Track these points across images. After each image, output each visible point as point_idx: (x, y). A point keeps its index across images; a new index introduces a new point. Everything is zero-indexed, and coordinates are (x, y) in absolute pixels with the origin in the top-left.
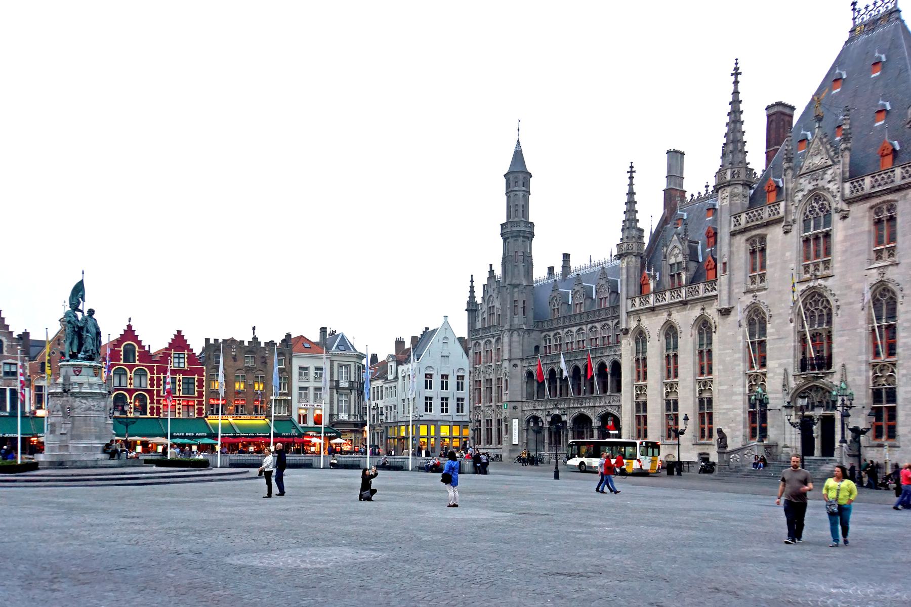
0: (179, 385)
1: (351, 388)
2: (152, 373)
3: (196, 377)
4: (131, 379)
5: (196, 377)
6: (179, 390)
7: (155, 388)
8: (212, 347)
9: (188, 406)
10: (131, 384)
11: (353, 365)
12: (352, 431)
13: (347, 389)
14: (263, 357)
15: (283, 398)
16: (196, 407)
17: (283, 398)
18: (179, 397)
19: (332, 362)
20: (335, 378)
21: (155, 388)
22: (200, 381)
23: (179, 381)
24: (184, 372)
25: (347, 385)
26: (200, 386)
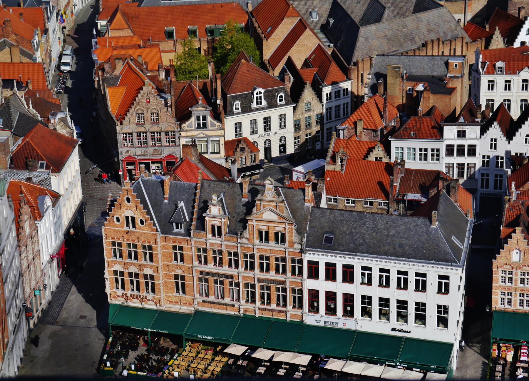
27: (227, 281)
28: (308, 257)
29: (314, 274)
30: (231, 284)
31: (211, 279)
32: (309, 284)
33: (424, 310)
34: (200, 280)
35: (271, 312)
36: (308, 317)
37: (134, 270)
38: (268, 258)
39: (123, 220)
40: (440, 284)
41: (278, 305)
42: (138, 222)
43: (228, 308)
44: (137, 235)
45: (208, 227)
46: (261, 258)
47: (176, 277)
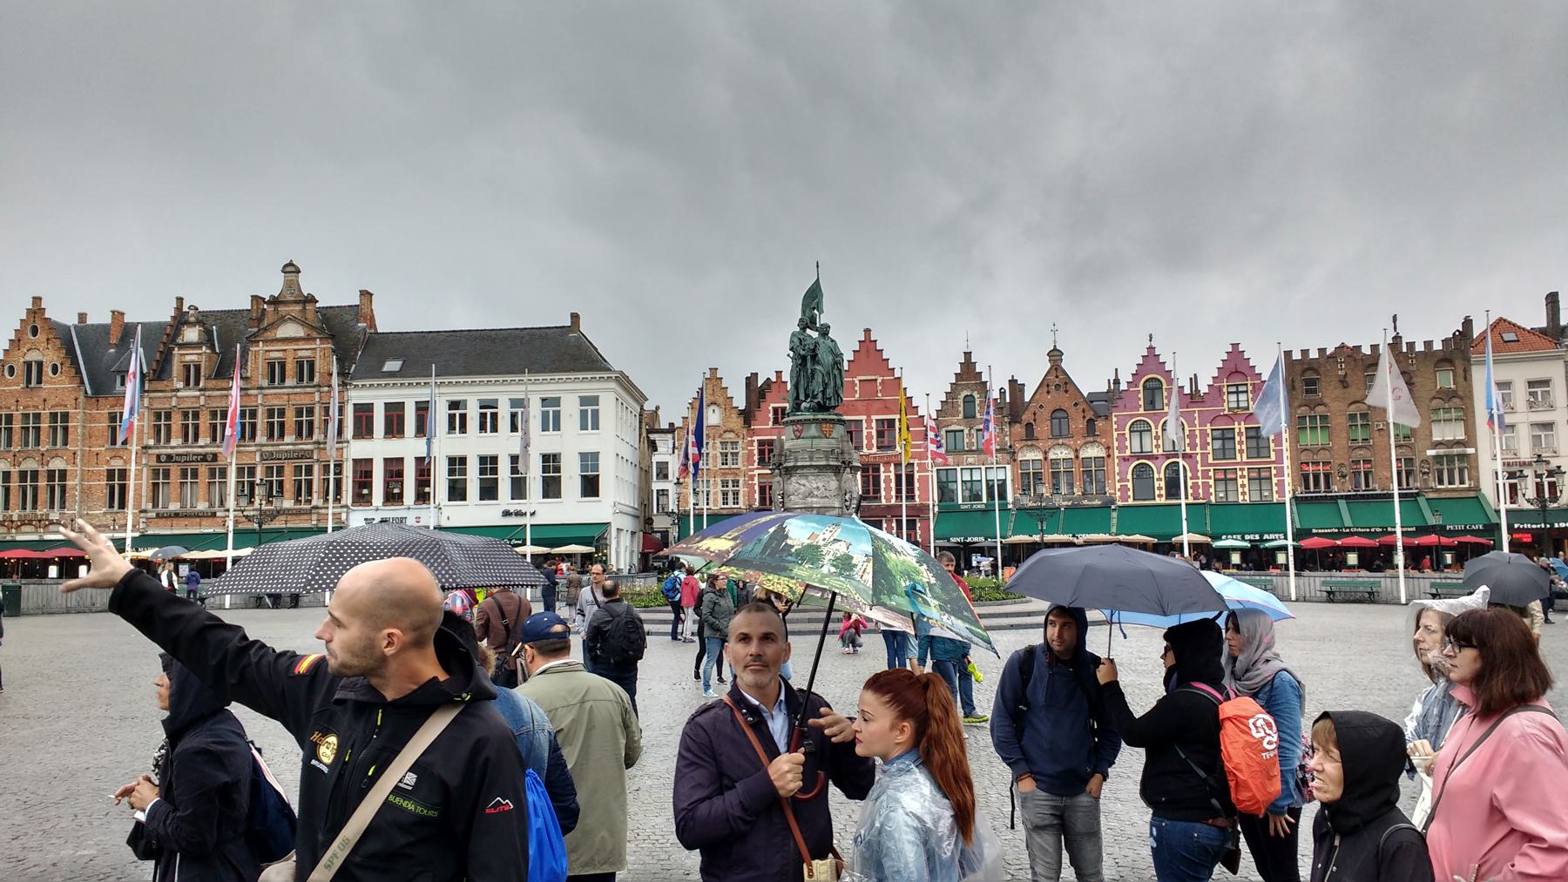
0: (1241, 443)
2: (1191, 424)
4: (1157, 438)
6: (1241, 451)
7: (1198, 450)
9: (1260, 479)
10: (1157, 446)
15: (1456, 450)
16: (1275, 480)
17: (1456, 450)
18: (1242, 463)
21: (1198, 450)
23: (1240, 434)
27: (203, 469)
28: (357, 396)
29: (364, 428)
30: (212, 473)
31: (175, 470)
32: (358, 449)
33: (557, 469)
34: (156, 473)
35: (283, 518)
36: (353, 516)
37: (29, 465)
38: (282, 413)
39: (20, 370)
40: (583, 414)
41: (298, 501)
42: (48, 370)
43: (205, 522)
44: (44, 394)
45: (176, 368)
46: (270, 413)
47: (110, 474)
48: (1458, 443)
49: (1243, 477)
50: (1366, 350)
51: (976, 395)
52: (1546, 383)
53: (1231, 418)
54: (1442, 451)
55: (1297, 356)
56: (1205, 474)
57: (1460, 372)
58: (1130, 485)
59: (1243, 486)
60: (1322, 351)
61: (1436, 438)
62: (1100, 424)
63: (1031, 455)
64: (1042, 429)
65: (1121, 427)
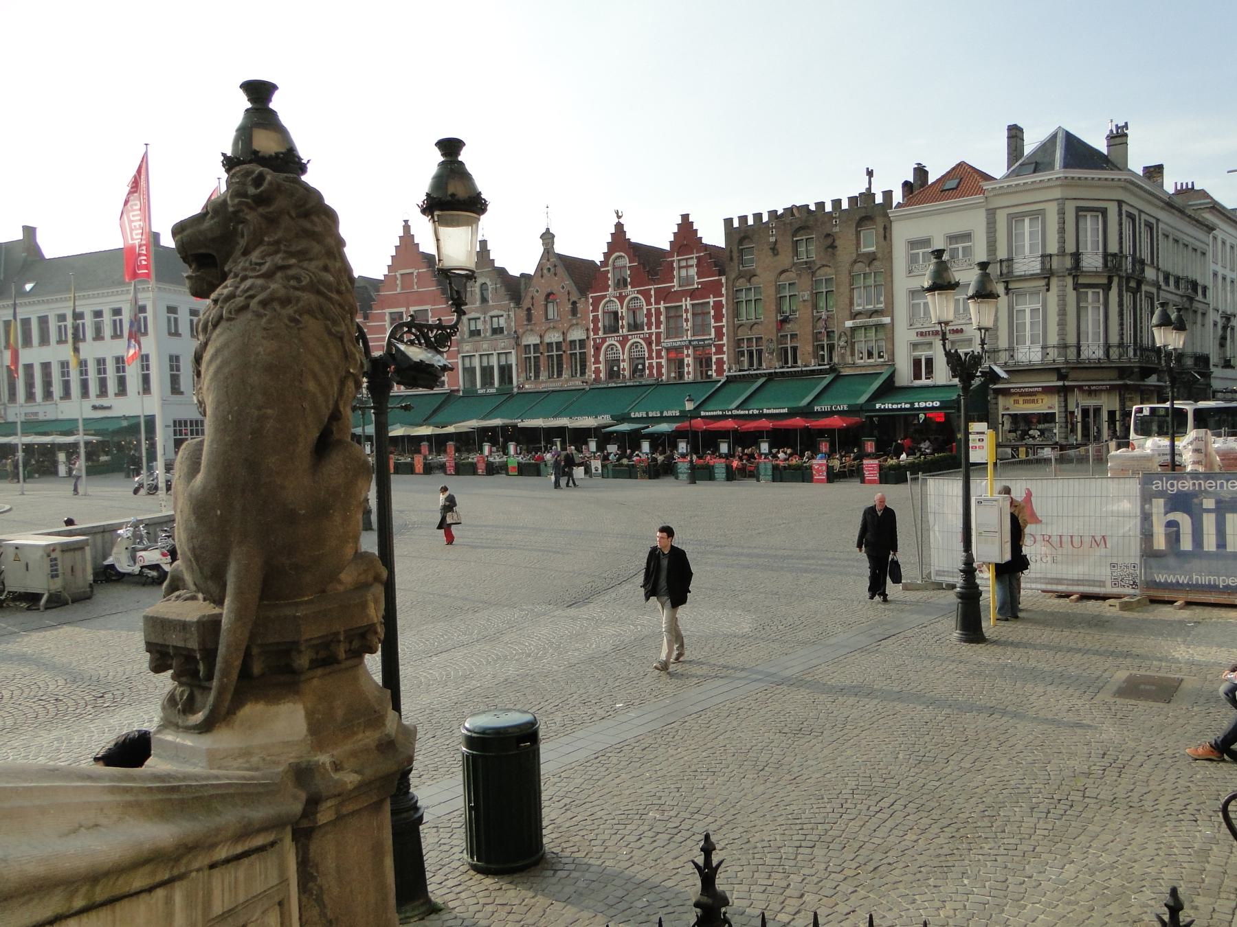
1: (1047, 275)
2: (649, 303)
3: (711, 300)
5: (711, 300)
7: (654, 330)
8: (743, 234)
11: (1052, 211)
12: (1048, 390)
13: (1033, 277)
14: (828, 235)
15: (874, 320)
17: (874, 320)
19: (991, 214)
20: (1002, 254)
21: (654, 330)
22: (718, 306)
24: (693, 294)
25: (1035, 267)
26: (718, 317)
36: (9, 411)
48: (875, 312)
49: (688, 356)
50: (812, 208)
51: (489, 283)
52: (967, 236)
53: (679, 295)
54: (858, 322)
55: (736, 224)
56: (659, 356)
57: (881, 230)
58: (602, 367)
59: (688, 365)
60: (758, 216)
61: (857, 308)
62: (580, 306)
63: (532, 340)
64: (537, 313)
65: (595, 309)
